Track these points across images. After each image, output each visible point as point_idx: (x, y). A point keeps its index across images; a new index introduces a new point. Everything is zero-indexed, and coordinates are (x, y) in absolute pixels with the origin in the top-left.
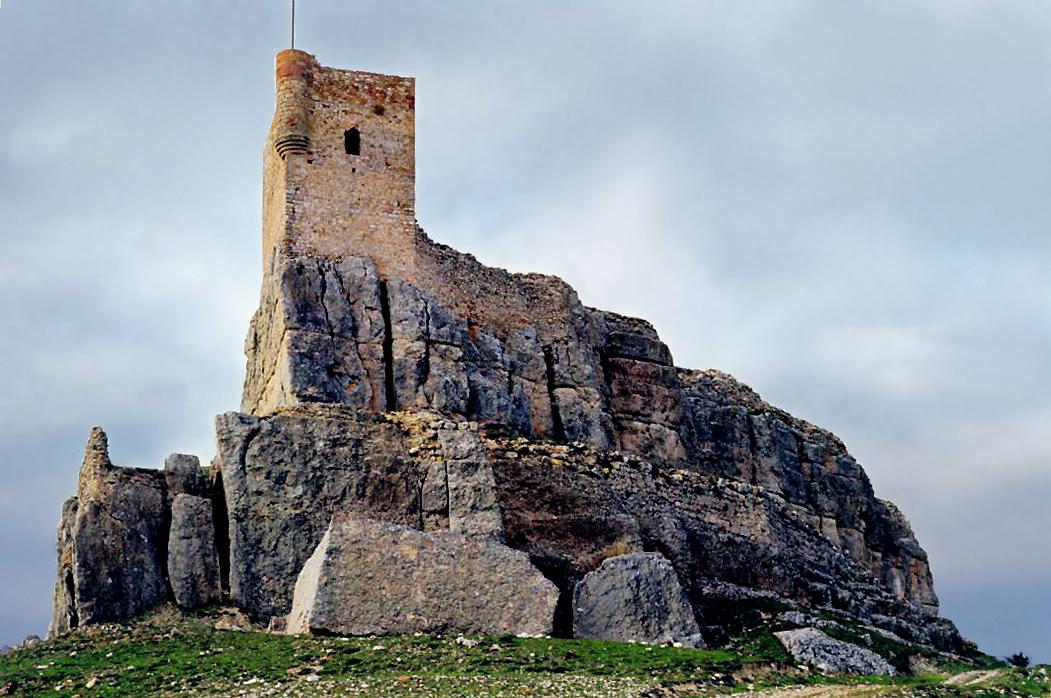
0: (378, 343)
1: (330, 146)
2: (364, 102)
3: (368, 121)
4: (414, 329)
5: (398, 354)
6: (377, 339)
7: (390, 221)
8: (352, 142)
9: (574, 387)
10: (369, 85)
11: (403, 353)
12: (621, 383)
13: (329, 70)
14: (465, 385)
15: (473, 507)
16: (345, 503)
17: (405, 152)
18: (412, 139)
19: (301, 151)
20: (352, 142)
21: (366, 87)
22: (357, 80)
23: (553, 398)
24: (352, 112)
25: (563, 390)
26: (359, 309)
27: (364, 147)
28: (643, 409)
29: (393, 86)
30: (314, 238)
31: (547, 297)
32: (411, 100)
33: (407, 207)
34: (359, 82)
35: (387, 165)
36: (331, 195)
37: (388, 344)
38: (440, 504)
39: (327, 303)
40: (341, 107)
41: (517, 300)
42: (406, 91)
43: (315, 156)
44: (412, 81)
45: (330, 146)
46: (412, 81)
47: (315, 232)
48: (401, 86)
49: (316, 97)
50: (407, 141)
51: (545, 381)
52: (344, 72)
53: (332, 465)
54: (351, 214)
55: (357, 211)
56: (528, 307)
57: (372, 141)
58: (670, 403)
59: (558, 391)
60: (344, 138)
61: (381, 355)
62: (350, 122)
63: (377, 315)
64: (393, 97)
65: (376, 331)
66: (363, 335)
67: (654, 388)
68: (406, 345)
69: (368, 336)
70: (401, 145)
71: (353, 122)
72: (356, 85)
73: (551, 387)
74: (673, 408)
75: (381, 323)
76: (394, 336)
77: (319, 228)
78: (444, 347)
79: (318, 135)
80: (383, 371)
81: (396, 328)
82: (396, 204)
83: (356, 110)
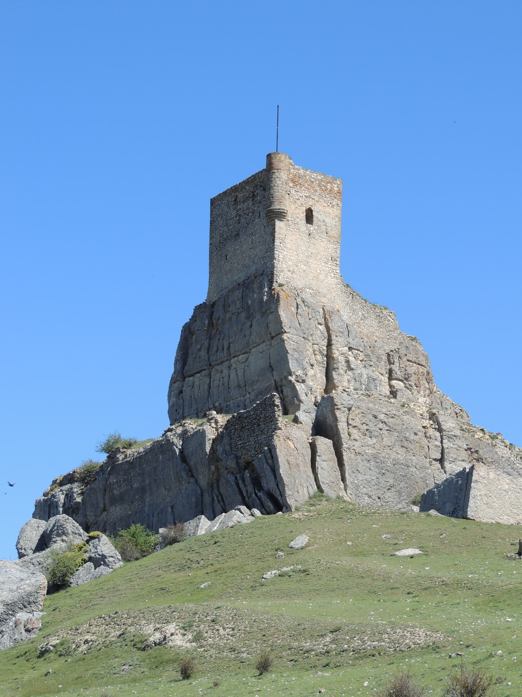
1: (298, 218)
2: (316, 191)
5: (336, 354)
8: (309, 217)
9: (402, 381)
14: (365, 376)
16: (394, 449)
20: (309, 217)
21: (317, 182)
22: (313, 176)
23: (391, 386)
24: (309, 197)
27: (315, 219)
30: (289, 274)
31: (387, 322)
37: (329, 345)
39: (299, 317)
45: (298, 218)
47: (289, 271)
51: (387, 375)
53: (388, 428)
54: (308, 262)
57: (319, 217)
58: (428, 392)
59: (394, 382)
60: (305, 214)
61: (325, 353)
62: (309, 203)
63: (322, 328)
65: (323, 338)
68: (339, 350)
70: (334, 221)
71: (310, 203)
72: (312, 180)
73: (390, 378)
75: (326, 334)
76: (333, 342)
78: (356, 351)
80: (325, 363)
82: (330, 258)
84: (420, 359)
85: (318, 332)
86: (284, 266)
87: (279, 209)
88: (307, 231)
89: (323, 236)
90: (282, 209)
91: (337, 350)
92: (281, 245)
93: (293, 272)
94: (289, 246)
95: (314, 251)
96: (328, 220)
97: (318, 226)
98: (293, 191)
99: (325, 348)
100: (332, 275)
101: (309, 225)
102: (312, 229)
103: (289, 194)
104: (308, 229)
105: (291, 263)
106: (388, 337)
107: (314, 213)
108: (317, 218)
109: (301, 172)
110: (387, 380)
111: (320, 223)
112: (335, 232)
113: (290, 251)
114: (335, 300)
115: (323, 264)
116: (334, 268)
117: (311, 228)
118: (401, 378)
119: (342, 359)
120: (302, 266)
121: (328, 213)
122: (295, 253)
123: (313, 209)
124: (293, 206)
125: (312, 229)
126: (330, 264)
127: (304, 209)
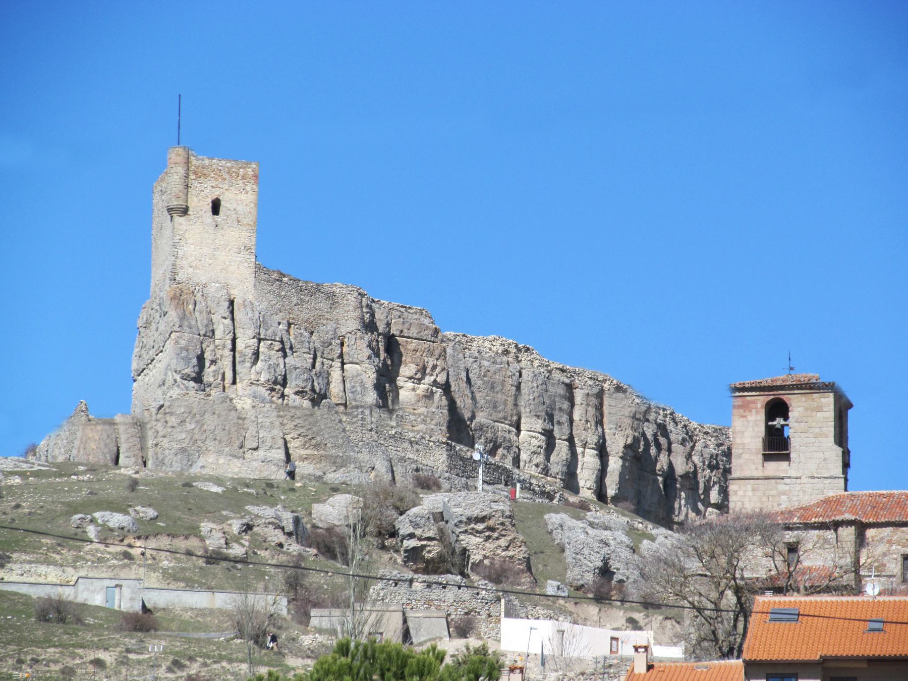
4: (251, 332)
8: (216, 207)
11: (243, 346)
15: (271, 447)
20: (216, 207)
25: (351, 365)
26: (216, 318)
30: (191, 270)
36: (202, 243)
38: (254, 445)
40: (210, 184)
43: (192, 217)
57: (229, 206)
61: (230, 346)
63: (228, 321)
66: (218, 334)
68: (245, 342)
79: (193, 202)
85: (222, 327)
93: (196, 268)
94: (190, 241)
96: (239, 208)
99: (230, 342)
109: (207, 162)
110: (339, 364)
111: (229, 212)
112: (250, 219)
118: (355, 360)
119: (249, 352)
121: (241, 199)
124: (196, 200)
127: (209, 201)
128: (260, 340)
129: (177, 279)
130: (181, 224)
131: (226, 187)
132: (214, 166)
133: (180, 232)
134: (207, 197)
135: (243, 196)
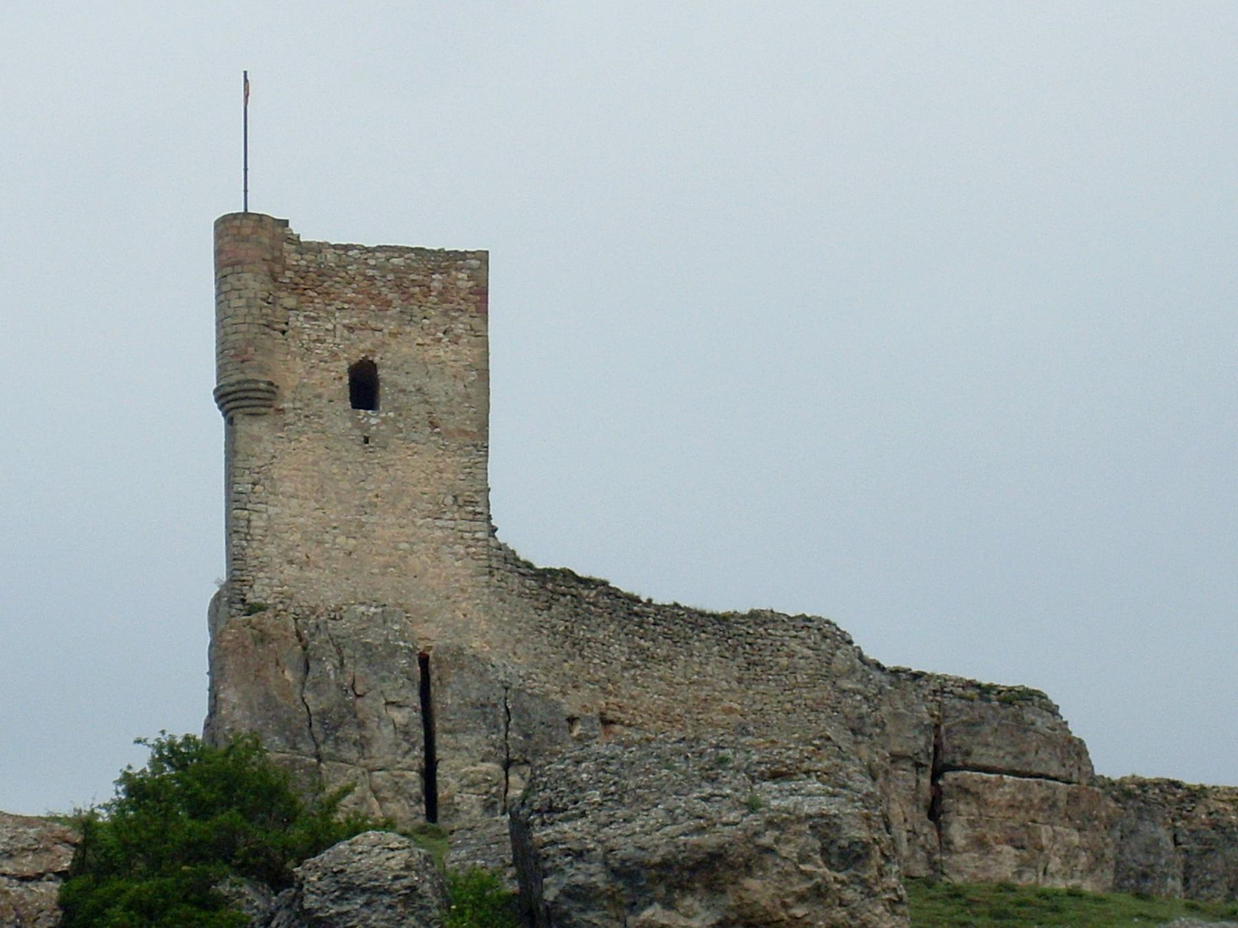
0: (410, 769)
2: (388, 304)
3: (393, 342)
6: (408, 760)
7: (438, 533)
8: (364, 387)
10: (395, 270)
12: (972, 824)
13: (319, 248)
17: (468, 397)
18: (484, 375)
19: (263, 410)
20: (364, 387)
21: (390, 277)
22: (372, 262)
24: (364, 326)
27: (385, 391)
28: (1019, 874)
29: (445, 271)
30: (291, 571)
31: (784, 661)
32: (481, 292)
33: (473, 503)
34: (374, 267)
35: (433, 425)
36: (321, 490)
41: (717, 670)
42: (470, 278)
43: (290, 417)
44: (483, 257)
45: (319, 396)
46: (483, 257)
47: (291, 562)
48: (459, 269)
49: (290, 302)
50: (473, 376)
52: (347, 248)
54: (361, 525)
55: (373, 519)
56: (740, 681)
57: (402, 380)
58: (1084, 859)
60: (346, 380)
61: (417, 789)
64: (448, 286)
65: (405, 746)
67: (1045, 833)
69: (389, 757)
70: (460, 387)
71: (367, 345)
72: (370, 272)
74: (1091, 870)
76: (440, 753)
77: (299, 554)
81: (441, 739)
82: (449, 500)
83: (372, 323)
84: (1031, 756)
85: (387, 731)
86: (271, 549)
87: (239, 382)
88: (358, 432)
89: (415, 437)
90: (248, 381)
91: (453, 776)
92: (258, 488)
93: (305, 564)
95: (385, 487)
96: (436, 386)
97: (396, 409)
98: (297, 321)
99: (413, 775)
100: (460, 549)
101: (362, 411)
102: (373, 421)
103: (284, 332)
104: (358, 425)
105: (297, 536)
106: (788, 706)
107: (382, 373)
108: (394, 385)
111: (403, 399)
113: (294, 502)
114: (467, 624)
115: (420, 522)
116: (465, 525)
117: (372, 419)
120: (341, 540)
122: (313, 504)
123: (376, 360)
124: (299, 366)
125: (373, 421)
126: (449, 515)
127: (344, 366)
128: (507, 765)
129: (250, 597)
130: (259, 439)
131: (393, 327)
132: (352, 269)
133: (255, 462)
134: (334, 355)
135: (443, 352)
